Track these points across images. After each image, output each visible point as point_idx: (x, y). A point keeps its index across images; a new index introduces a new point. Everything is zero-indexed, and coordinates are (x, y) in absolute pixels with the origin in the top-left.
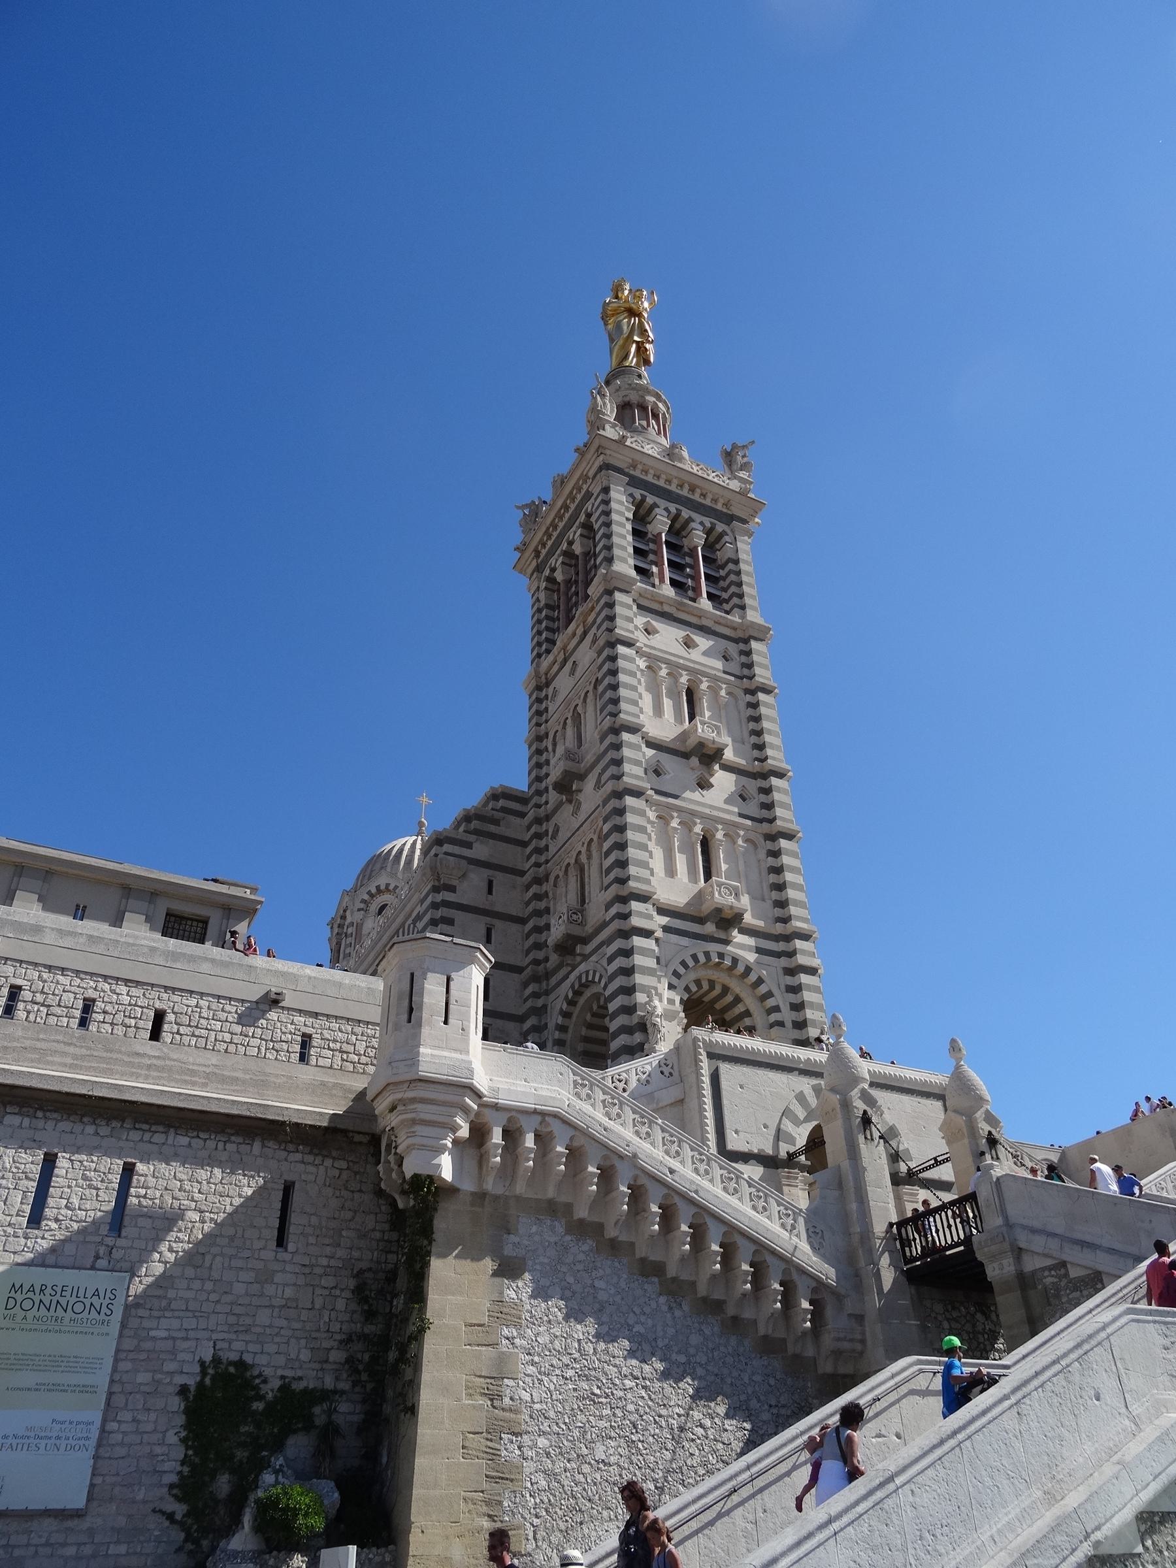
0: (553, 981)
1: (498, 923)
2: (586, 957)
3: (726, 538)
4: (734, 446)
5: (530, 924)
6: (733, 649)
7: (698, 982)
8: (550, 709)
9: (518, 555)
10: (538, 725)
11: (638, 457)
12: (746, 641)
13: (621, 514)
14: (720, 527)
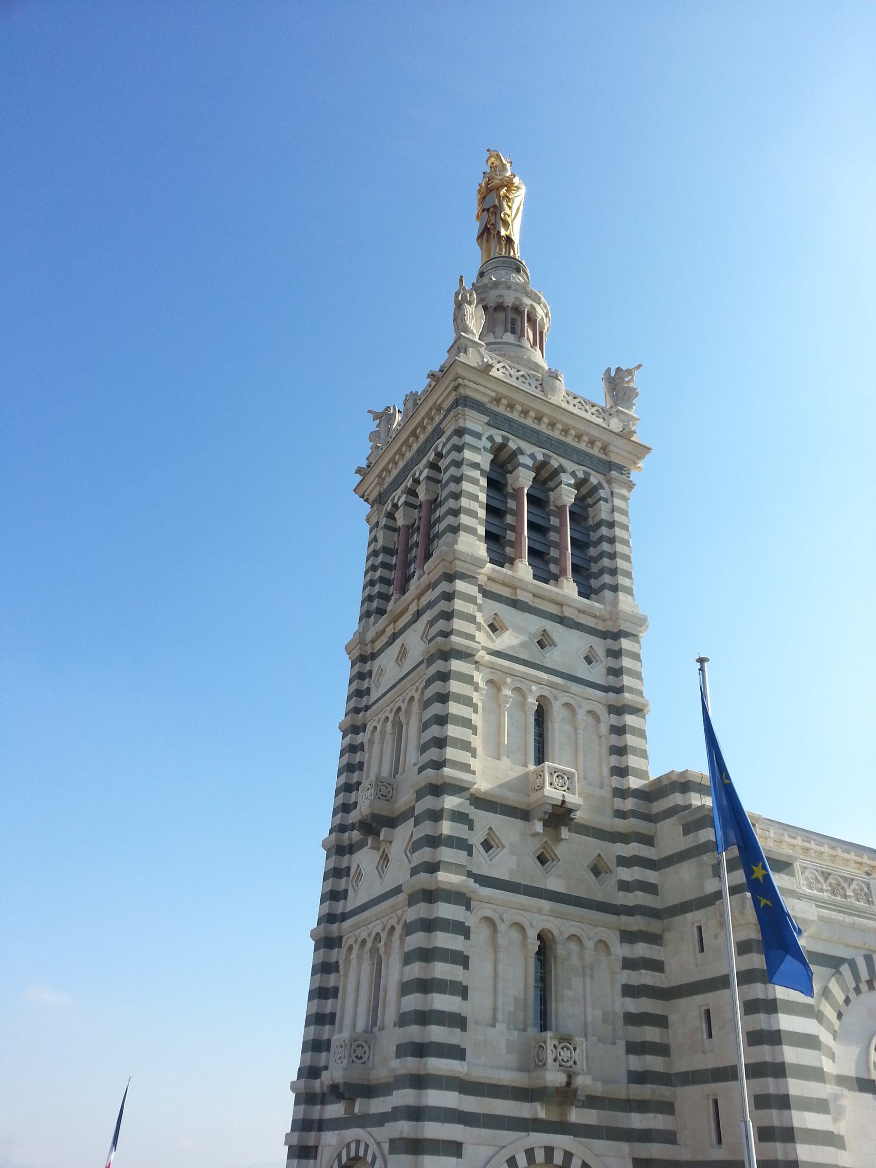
3: (602, 493)
4: (618, 370)
6: (600, 646)
8: (373, 690)
9: (359, 478)
10: (356, 710)
11: (503, 390)
12: (617, 636)
13: (476, 466)
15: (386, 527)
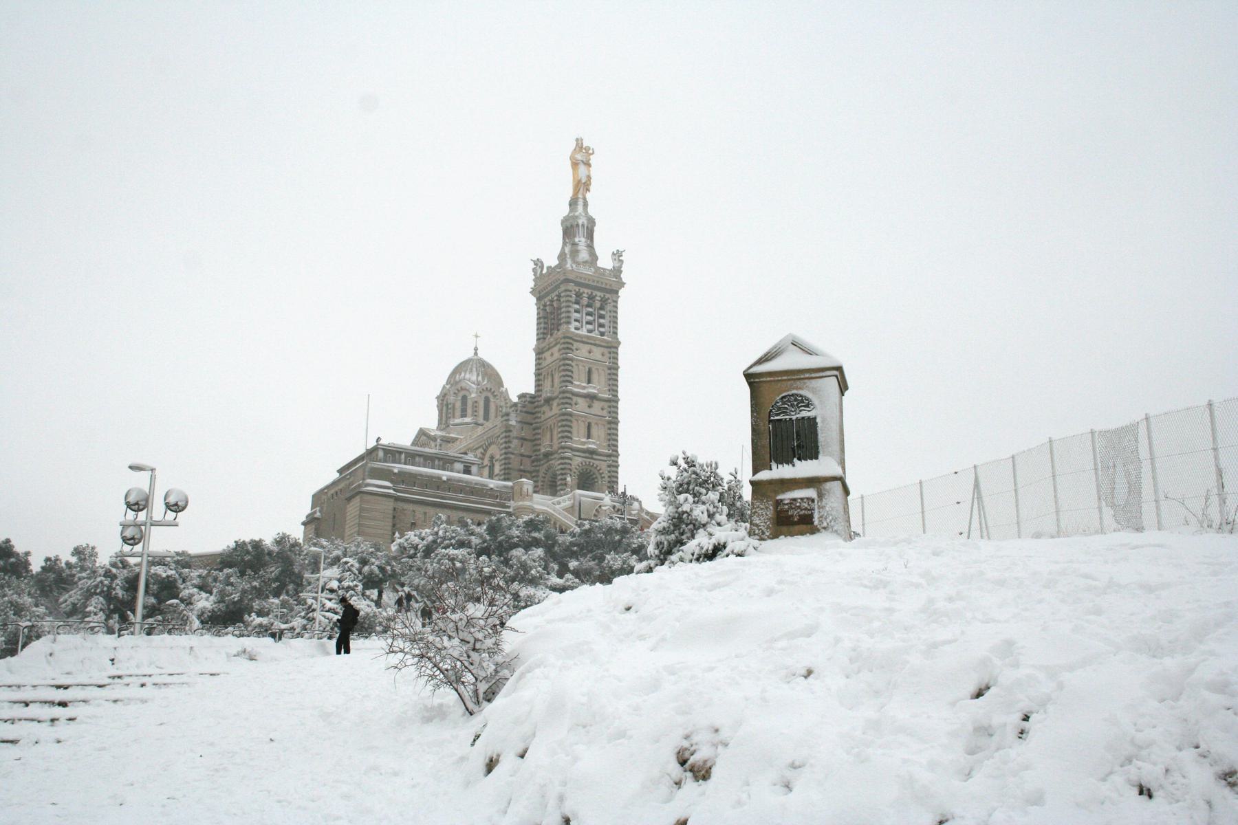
0: (542, 462)
1: (525, 442)
2: (552, 460)
3: (609, 301)
4: (618, 250)
5: (534, 443)
6: (606, 351)
7: (583, 470)
12: (610, 347)
14: (608, 296)
15: (542, 310)
